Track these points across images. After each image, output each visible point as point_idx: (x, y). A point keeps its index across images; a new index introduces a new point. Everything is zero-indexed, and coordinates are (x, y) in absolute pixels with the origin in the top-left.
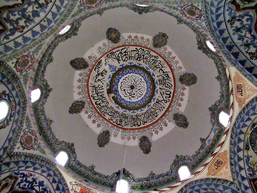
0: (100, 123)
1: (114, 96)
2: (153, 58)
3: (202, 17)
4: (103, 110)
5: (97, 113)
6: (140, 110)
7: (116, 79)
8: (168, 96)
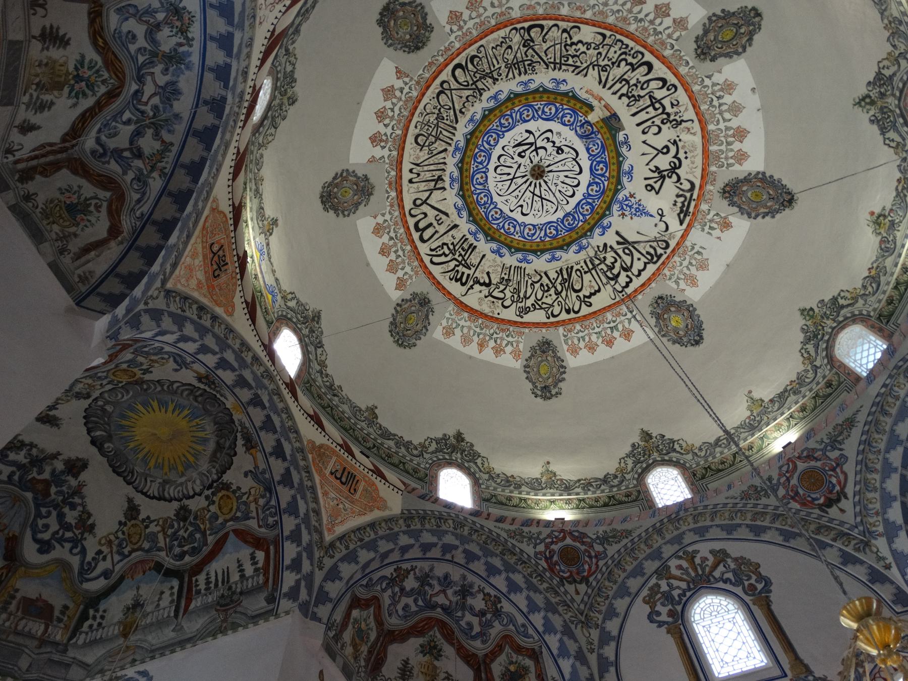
1: (586, 114)
2: (529, 303)
3: (545, 565)
4: (615, 52)
5: (637, 34)
6: (478, 117)
7: (603, 175)
8: (422, 225)
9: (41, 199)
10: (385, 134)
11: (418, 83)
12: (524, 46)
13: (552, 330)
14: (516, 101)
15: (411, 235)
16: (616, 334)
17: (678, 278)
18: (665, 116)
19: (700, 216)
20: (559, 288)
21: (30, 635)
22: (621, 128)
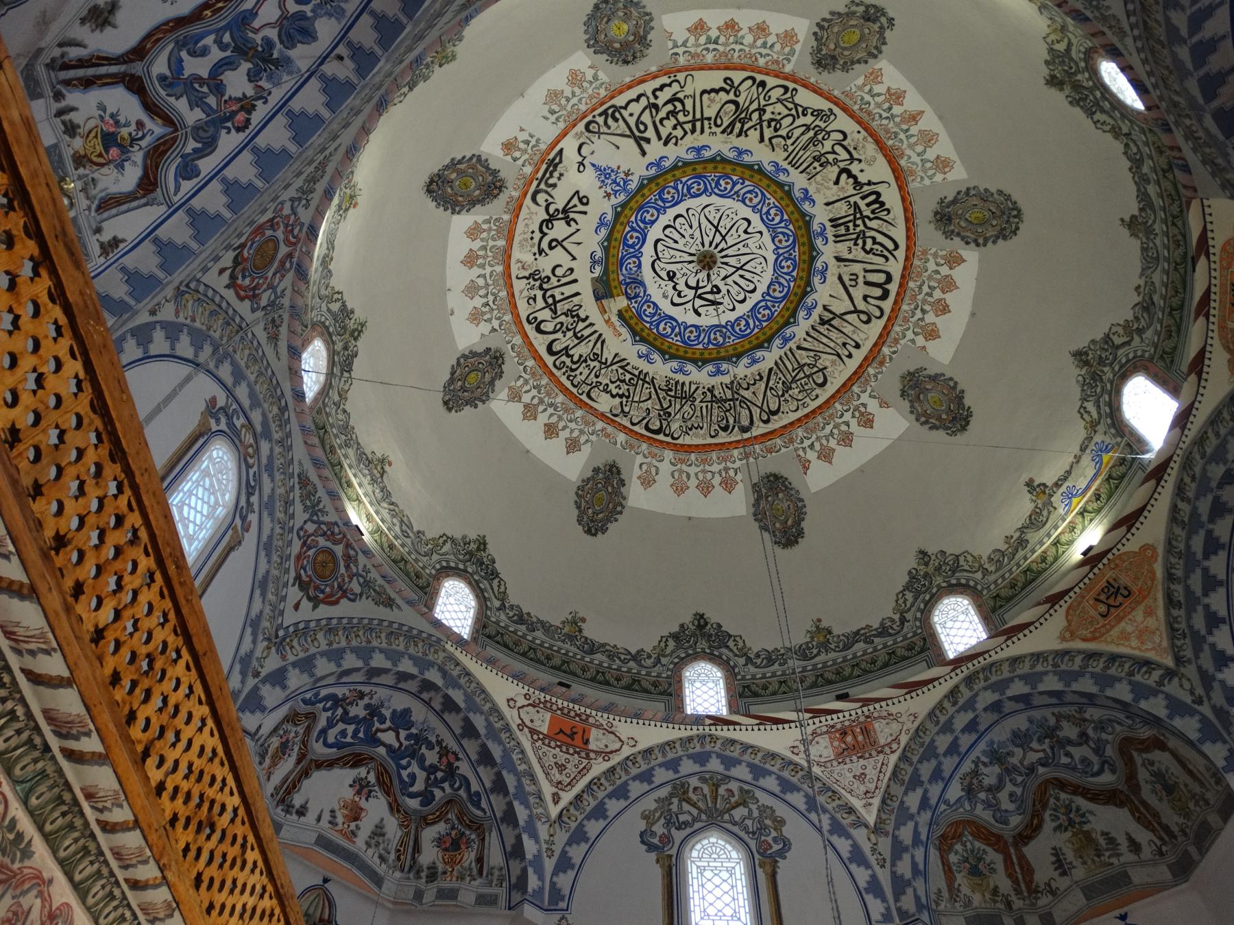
0: (576, 434)
1: (628, 309)
2: (808, 119)
5: (557, 391)
6: (745, 361)
7: (633, 229)
8: (878, 292)
10: (853, 417)
11: (791, 441)
12: (670, 414)
13: (801, 75)
14: (698, 355)
15: (898, 294)
16: (714, 34)
17: (591, 83)
18: (545, 286)
19: (536, 158)
20: (755, 116)
22: (594, 280)
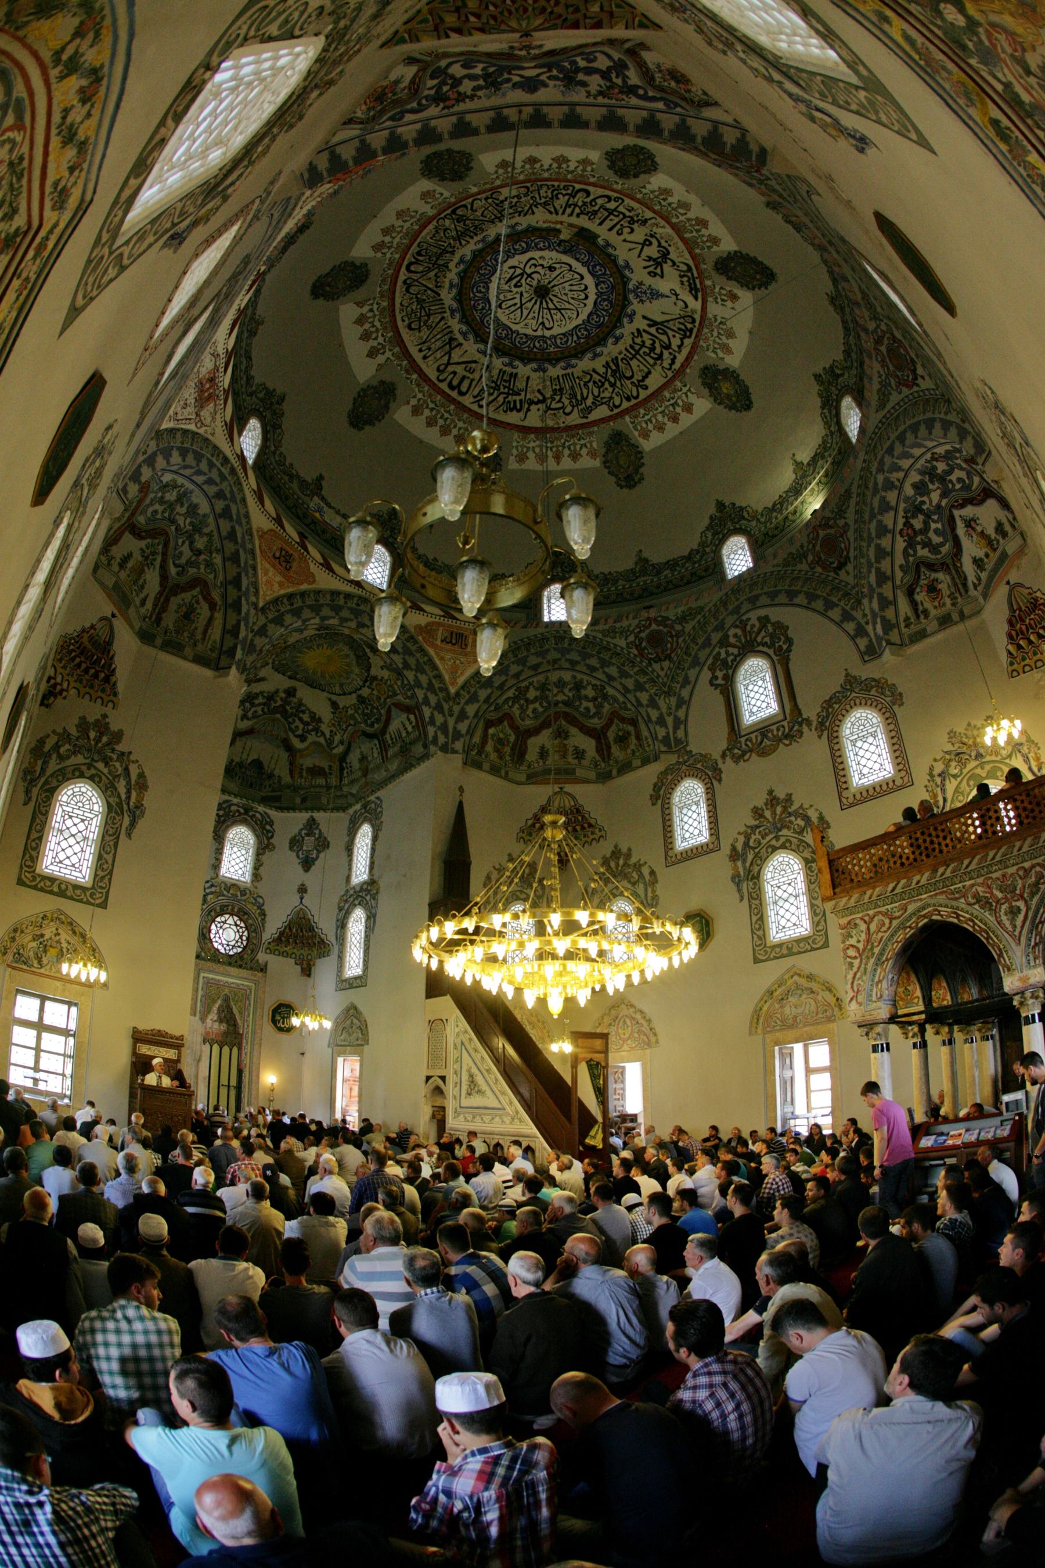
2: (589, 402)
6: (456, 281)
8: (455, 383)
9: (171, 627)
11: (382, 296)
13: (619, 420)
16: (678, 410)
20: (612, 380)
21: (321, 787)
